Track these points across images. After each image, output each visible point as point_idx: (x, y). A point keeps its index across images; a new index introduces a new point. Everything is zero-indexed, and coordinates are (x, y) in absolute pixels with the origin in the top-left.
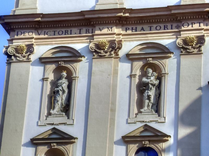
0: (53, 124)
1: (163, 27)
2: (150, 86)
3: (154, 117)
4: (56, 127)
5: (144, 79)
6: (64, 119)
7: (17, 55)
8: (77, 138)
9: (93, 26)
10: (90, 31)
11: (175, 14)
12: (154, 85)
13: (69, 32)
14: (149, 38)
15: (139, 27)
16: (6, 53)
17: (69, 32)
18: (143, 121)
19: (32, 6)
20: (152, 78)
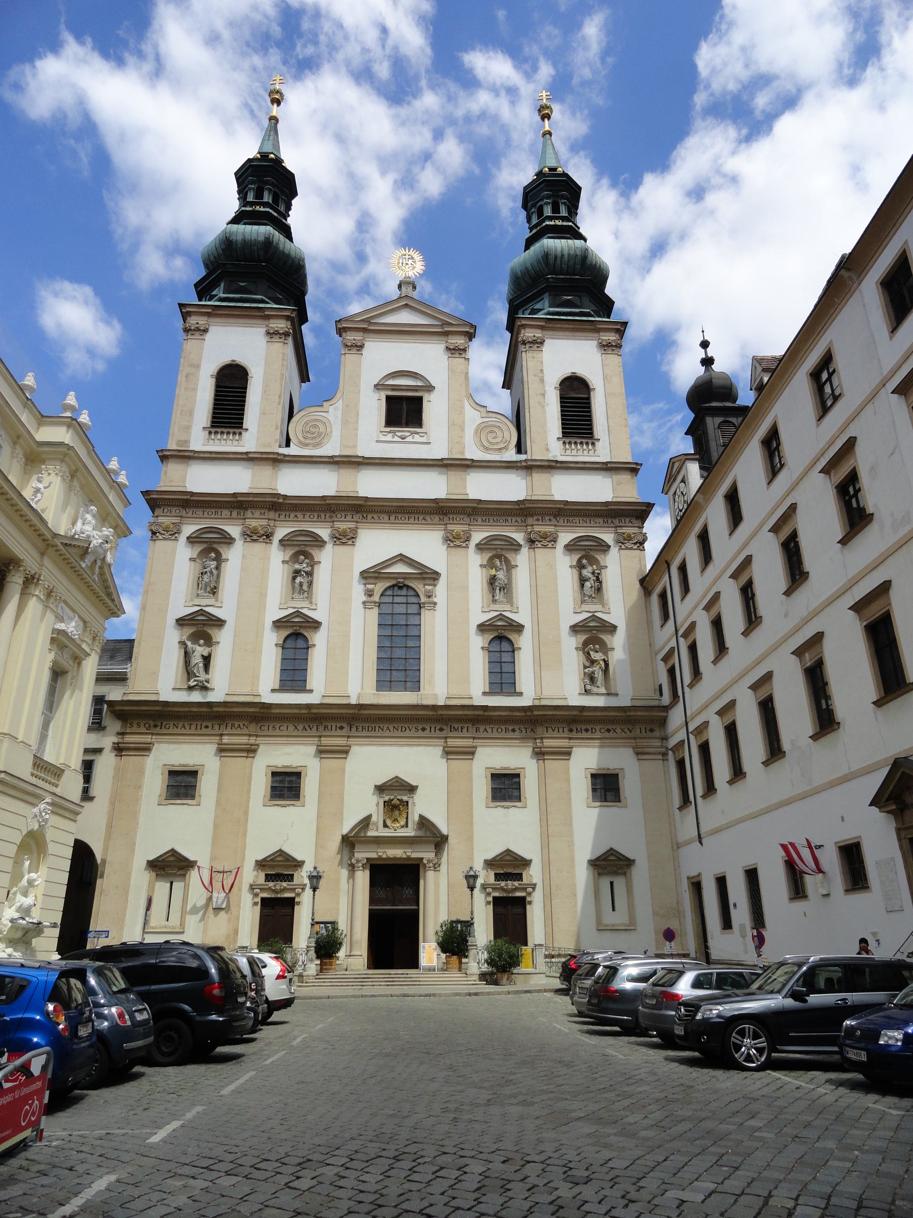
2: (303, 573)
3: (305, 604)
5: (297, 566)
6: (211, 601)
7: (163, 532)
8: (224, 622)
9: (246, 509)
10: (242, 514)
11: (329, 504)
12: (306, 573)
13: (219, 514)
15: (292, 515)
16: (151, 530)
17: (219, 514)
18: (295, 608)
19: (181, 484)
20: (305, 565)
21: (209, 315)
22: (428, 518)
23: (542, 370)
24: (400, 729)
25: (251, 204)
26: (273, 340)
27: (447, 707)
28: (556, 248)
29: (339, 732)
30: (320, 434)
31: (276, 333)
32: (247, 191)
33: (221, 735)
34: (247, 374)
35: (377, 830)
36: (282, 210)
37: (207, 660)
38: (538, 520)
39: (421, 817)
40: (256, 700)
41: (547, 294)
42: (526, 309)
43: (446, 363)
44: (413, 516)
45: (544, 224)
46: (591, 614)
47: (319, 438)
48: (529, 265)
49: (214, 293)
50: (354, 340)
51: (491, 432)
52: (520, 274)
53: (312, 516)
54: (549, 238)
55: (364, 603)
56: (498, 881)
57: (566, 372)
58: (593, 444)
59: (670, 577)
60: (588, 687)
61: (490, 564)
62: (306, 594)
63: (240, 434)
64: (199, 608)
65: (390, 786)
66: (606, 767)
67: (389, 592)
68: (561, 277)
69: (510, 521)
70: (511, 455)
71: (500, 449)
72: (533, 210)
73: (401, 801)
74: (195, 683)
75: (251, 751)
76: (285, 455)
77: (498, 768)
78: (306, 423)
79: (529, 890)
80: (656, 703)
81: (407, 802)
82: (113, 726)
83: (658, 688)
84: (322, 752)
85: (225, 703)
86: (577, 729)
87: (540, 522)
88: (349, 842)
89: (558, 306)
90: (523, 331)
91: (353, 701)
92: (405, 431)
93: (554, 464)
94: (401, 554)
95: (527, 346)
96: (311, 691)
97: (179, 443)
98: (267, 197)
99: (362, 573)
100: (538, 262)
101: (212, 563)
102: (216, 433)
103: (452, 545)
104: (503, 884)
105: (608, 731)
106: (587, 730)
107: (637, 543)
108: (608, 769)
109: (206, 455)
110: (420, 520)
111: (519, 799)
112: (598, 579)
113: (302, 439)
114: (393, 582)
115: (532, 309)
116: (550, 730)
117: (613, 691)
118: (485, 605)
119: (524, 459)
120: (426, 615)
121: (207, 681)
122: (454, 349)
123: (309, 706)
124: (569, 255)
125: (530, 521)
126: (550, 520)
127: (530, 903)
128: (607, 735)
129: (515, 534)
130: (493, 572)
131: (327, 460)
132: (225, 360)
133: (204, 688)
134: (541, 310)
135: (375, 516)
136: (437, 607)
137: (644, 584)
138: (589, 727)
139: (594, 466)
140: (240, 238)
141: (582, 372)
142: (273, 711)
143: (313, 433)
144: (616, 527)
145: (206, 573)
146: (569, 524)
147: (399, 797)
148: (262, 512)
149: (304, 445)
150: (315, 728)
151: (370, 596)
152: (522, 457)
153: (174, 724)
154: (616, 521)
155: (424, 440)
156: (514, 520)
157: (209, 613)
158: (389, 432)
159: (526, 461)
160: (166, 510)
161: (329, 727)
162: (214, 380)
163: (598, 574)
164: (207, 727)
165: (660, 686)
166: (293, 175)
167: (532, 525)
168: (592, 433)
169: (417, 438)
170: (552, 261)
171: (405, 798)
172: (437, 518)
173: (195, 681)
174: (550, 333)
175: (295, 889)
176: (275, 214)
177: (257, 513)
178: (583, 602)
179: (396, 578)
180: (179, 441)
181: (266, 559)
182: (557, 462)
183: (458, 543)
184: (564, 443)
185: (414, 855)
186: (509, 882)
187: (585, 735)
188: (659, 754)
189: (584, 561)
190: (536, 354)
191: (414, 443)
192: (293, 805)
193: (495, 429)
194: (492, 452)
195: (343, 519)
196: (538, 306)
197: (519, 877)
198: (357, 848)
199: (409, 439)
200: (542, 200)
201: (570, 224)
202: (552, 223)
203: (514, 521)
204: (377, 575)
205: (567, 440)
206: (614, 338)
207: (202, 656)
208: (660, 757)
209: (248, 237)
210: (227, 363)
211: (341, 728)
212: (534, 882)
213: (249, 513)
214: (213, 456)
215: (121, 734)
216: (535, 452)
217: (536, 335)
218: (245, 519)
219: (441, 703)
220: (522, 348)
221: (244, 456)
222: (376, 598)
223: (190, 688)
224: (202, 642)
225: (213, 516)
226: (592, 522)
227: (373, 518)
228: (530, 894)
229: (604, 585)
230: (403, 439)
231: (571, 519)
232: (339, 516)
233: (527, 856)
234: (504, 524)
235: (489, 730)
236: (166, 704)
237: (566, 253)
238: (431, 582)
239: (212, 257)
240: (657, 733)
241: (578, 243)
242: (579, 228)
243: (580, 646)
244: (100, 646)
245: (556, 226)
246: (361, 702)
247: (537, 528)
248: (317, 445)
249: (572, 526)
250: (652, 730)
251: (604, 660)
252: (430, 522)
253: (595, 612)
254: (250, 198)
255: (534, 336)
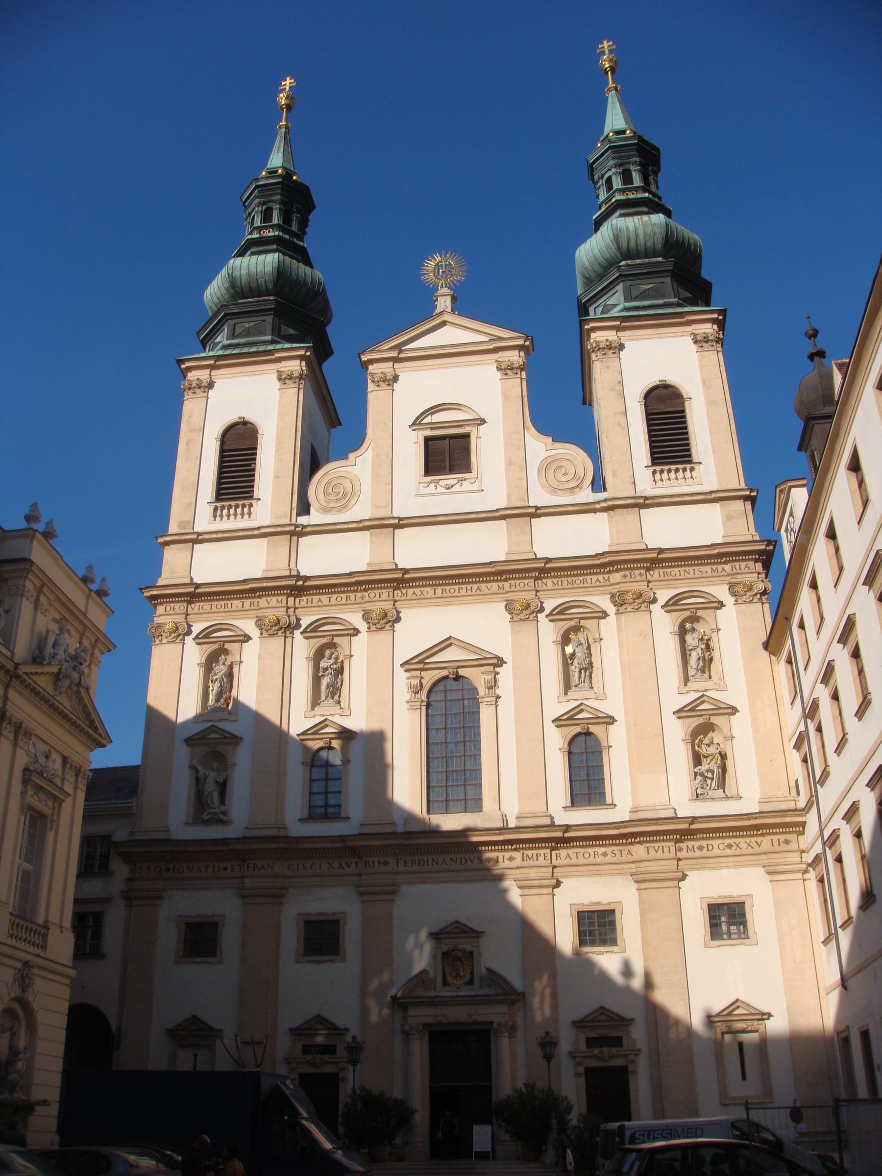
0: (211, 721)
1: (344, 599)
4: (217, 724)
13: (229, 606)
14: (328, 612)
17: (229, 606)
21: (212, 368)
22: (483, 586)
23: (621, 383)
24: (459, 861)
25: (259, 229)
26: (285, 386)
27: (518, 829)
28: (628, 230)
29: (383, 868)
30: (345, 494)
31: (290, 377)
32: (254, 215)
33: (242, 878)
34: (257, 432)
35: (435, 989)
36: (294, 229)
37: (223, 787)
38: (625, 576)
39: (488, 970)
40: (282, 833)
41: (621, 285)
42: (597, 307)
43: (498, 385)
44: (464, 586)
45: (614, 200)
46: (701, 694)
47: (345, 499)
48: (596, 251)
49: (217, 340)
50: (382, 373)
51: (560, 467)
52: (587, 264)
53: (339, 599)
54: (622, 215)
55: (408, 702)
56: (592, 1048)
57: (653, 380)
58: (692, 469)
59: (792, 639)
60: (699, 791)
61: (565, 640)
62: (336, 697)
63: (251, 505)
64: (210, 724)
65: (448, 933)
66: (727, 894)
67: (441, 687)
68: (638, 261)
69: (589, 582)
70: (586, 495)
71: (572, 488)
72: (600, 183)
73: (464, 951)
74: (209, 816)
75: (278, 895)
76: (304, 527)
77: (586, 903)
78: (328, 483)
79: (632, 1057)
80: (792, 806)
81: (471, 953)
82: (120, 870)
83: (793, 784)
84: (364, 893)
85: (244, 838)
86: (687, 846)
87: (628, 579)
88: (399, 1004)
89: (636, 299)
90: (593, 335)
91: (400, 829)
92: (450, 479)
93: (642, 501)
94: (450, 638)
95: (599, 354)
96: (347, 819)
97: (181, 525)
98: (276, 219)
99: (402, 665)
100: (608, 247)
101: (222, 667)
102: (223, 508)
103: (516, 618)
104: (596, 1051)
105: (730, 846)
106: (701, 848)
107: (756, 594)
108: (730, 897)
109: (214, 536)
110: (474, 590)
111: (613, 942)
112: (708, 647)
113: (324, 504)
114: (445, 673)
115: (605, 305)
116: (652, 851)
117: (735, 793)
118: (562, 693)
119: (603, 499)
120: (486, 714)
121: (224, 814)
122: (505, 369)
123: (342, 838)
124: (645, 234)
125: (616, 577)
126: (641, 575)
127: (634, 1073)
128: (728, 852)
129: (596, 597)
130: (569, 650)
131: (354, 526)
132: (231, 417)
133: (220, 820)
134: (615, 306)
135: (417, 590)
136: (500, 701)
137: (769, 648)
138: (704, 843)
139: (695, 498)
140: (244, 272)
141: (672, 379)
142: (302, 846)
143: (338, 494)
144: (729, 575)
145: (216, 680)
146: (666, 578)
147: (460, 947)
148: (279, 600)
149: (326, 510)
150: (354, 865)
151: (416, 693)
152: (602, 496)
153: (188, 867)
154: (727, 567)
155: (475, 487)
156: (594, 580)
157: (221, 729)
158: (431, 482)
159: (606, 500)
160: (168, 608)
161: (371, 864)
162: (219, 443)
163: (708, 640)
164: (225, 869)
165: (797, 782)
166: (306, 188)
167: (618, 583)
168: (690, 456)
169: (466, 485)
170: (624, 245)
171: (468, 948)
172: (494, 586)
173: (209, 813)
174: (628, 333)
175: (338, 1063)
176: (287, 237)
177: (273, 601)
178: (686, 680)
179: (445, 668)
180: (181, 522)
181: (286, 657)
182: (646, 498)
183: (523, 616)
184: (654, 472)
185: (481, 1019)
186: (605, 1050)
187: (698, 853)
188: (797, 871)
189: (688, 625)
190: (612, 362)
191: (462, 492)
192: (332, 961)
193: (564, 463)
194: (560, 493)
195: (377, 598)
196: (611, 301)
197: (618, 1041)
198: (412, 1011)
199: (456, 488)
200: (610, 170)
201: (647, 195)
202: (623, 197)
203: (594, 580)
204: (421, 666)
205: (658, 468)
206: (711, 331)
207: (217, 782)
208: (799, 876)
209: (253, 269)
210: (233, 421)
211: (386, 863)
212: (638, 1046)
213: (263, 602)
214: (220, 535)
215: (129, 880)
216: (616, 488)
217: (610, 339)
218: (260, 609)
219: (512, 824)
220: (593, 356)
221: (256, 532)
222: (423, 696)
223: (206, 823)
224: (215, 765)
225: (222, 609)
226: (697, 572)
227: (414, 593)
228: (633, 1062)
229: (716, 655)
230: (449, 488)
231: (669, 570)
232: (372, 595)
233: (627, 1014)
234: (581, 585)
235: (573, 856)
236: (178, 842)
237: (641, 232)
238: (491, 668)
239: (215, 300)
240: (793, 846)
241: (658, 218)
242: (660, 198)
243: (688, 737)
244: (85, 782)
245: (627, 200)
246: (408, 829)
247: (623, 587)
248: (343, 508)
249: (668, 582)
250: (787, 842)
251: (720, 753)
252: (486, 591)
253: (706, 690)
254: (258, 223)
255: (607, 340)
